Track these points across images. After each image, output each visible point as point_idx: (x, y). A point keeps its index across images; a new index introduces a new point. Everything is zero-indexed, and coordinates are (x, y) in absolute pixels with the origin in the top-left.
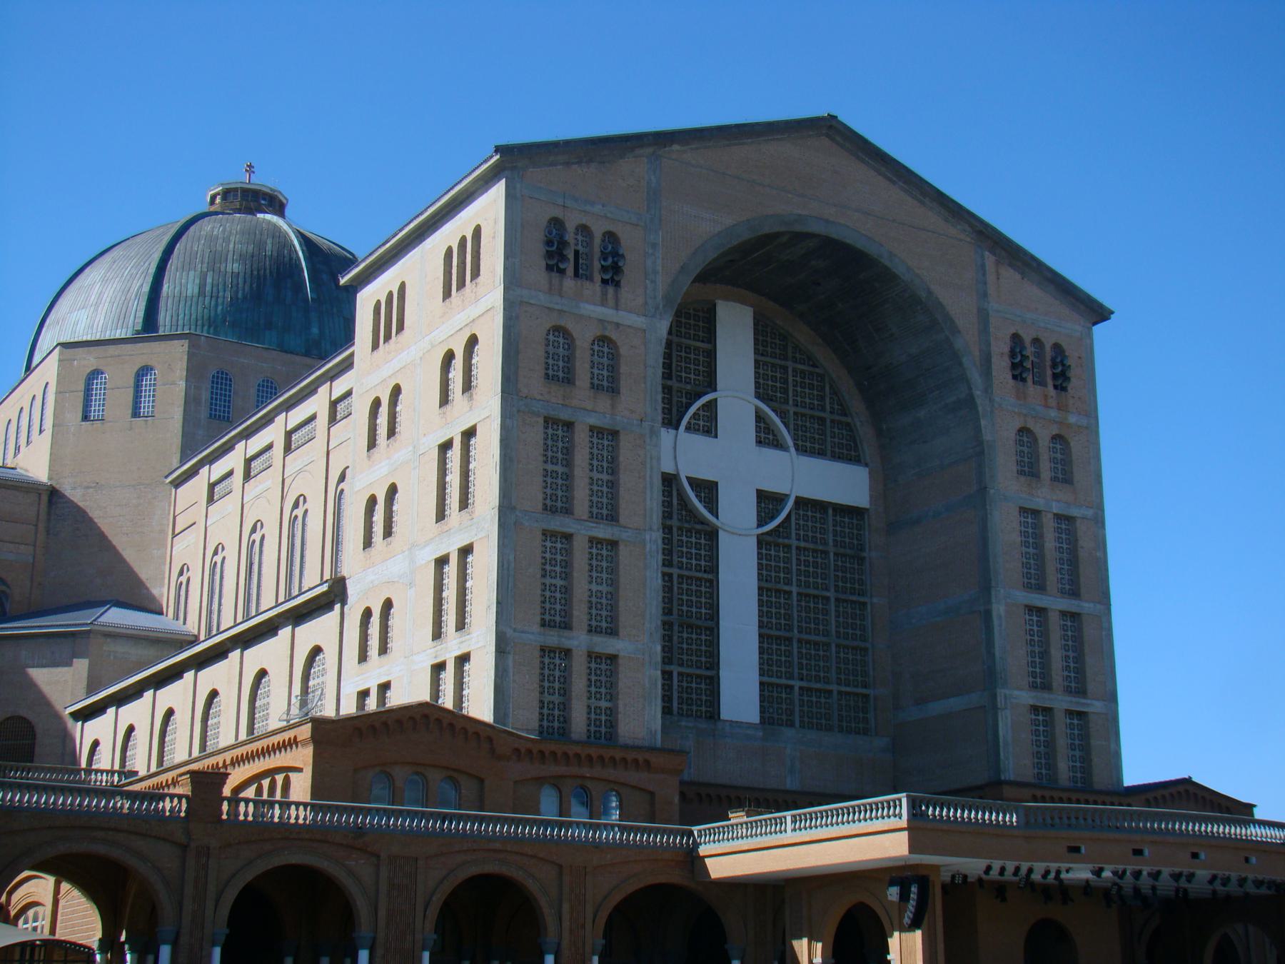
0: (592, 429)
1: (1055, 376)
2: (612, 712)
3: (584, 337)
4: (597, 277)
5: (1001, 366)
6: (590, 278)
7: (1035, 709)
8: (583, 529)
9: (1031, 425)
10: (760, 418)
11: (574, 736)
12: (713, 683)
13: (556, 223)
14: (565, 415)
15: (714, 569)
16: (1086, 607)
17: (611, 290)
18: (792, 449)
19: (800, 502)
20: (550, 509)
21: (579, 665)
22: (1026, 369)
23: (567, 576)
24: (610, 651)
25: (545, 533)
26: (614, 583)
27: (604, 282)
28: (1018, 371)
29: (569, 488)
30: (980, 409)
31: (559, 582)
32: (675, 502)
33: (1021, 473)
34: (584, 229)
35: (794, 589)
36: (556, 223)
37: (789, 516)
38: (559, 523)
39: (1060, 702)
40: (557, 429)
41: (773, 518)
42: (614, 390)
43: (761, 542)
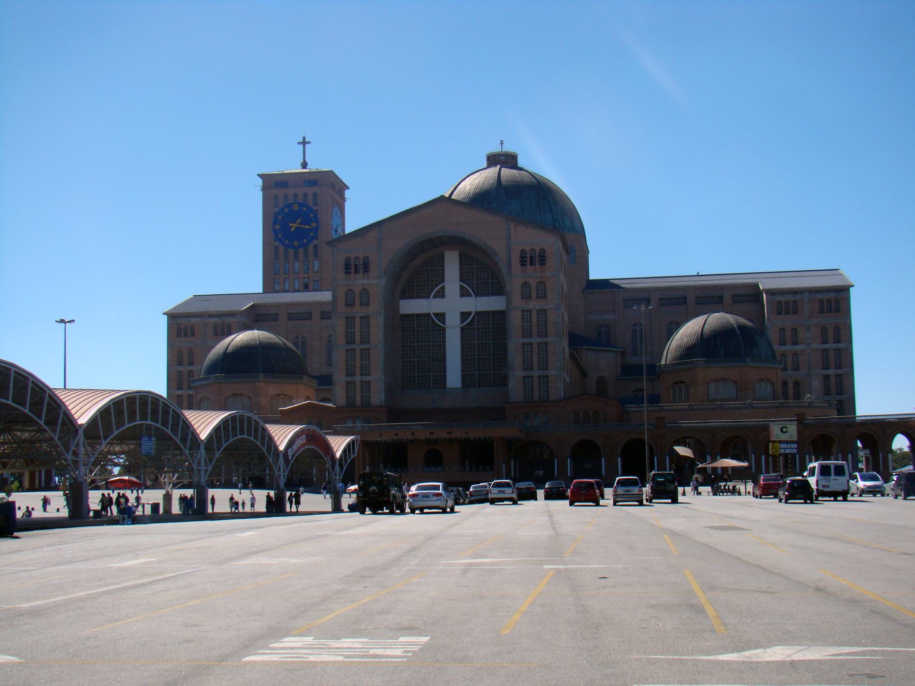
0: (361, 317)
1: (540, 260)
2: (370, 396)
3: (357, 291)
4: (361, 271)
5: (516, 263)
6: (359, 272)
7: (524, 377)
8: (358, 347)
9: (528, 280)
10: (462, 287)
11: (357, 405)
12: (445, 376)
13: (349, 258)
14: (352, 315)
15: (444, 341)
16: (550, 339)
17: (366, 274)
18: (474, 296)
19: (478, 313)
20: (347, 343)
21: (358, 385)
22: (526, 261)
23: (355, 361)
24: (368, 380)
25: (347, 350)
26: (369, 360)
27: (364, 272)
28: (523, 263)
29: (355, 335)
30: (506, 280)
31: (353, 363)
32: (430, 321)
33: (523, 298)
34: (357, 258)
35: (476, 342)
36: (349, 258)
37: (474, 318)
38: (350, 347)
39: (536, 373)
40: (350, 320)
41: (467, 319)
42: (368, 304)
43: (462, 329)
